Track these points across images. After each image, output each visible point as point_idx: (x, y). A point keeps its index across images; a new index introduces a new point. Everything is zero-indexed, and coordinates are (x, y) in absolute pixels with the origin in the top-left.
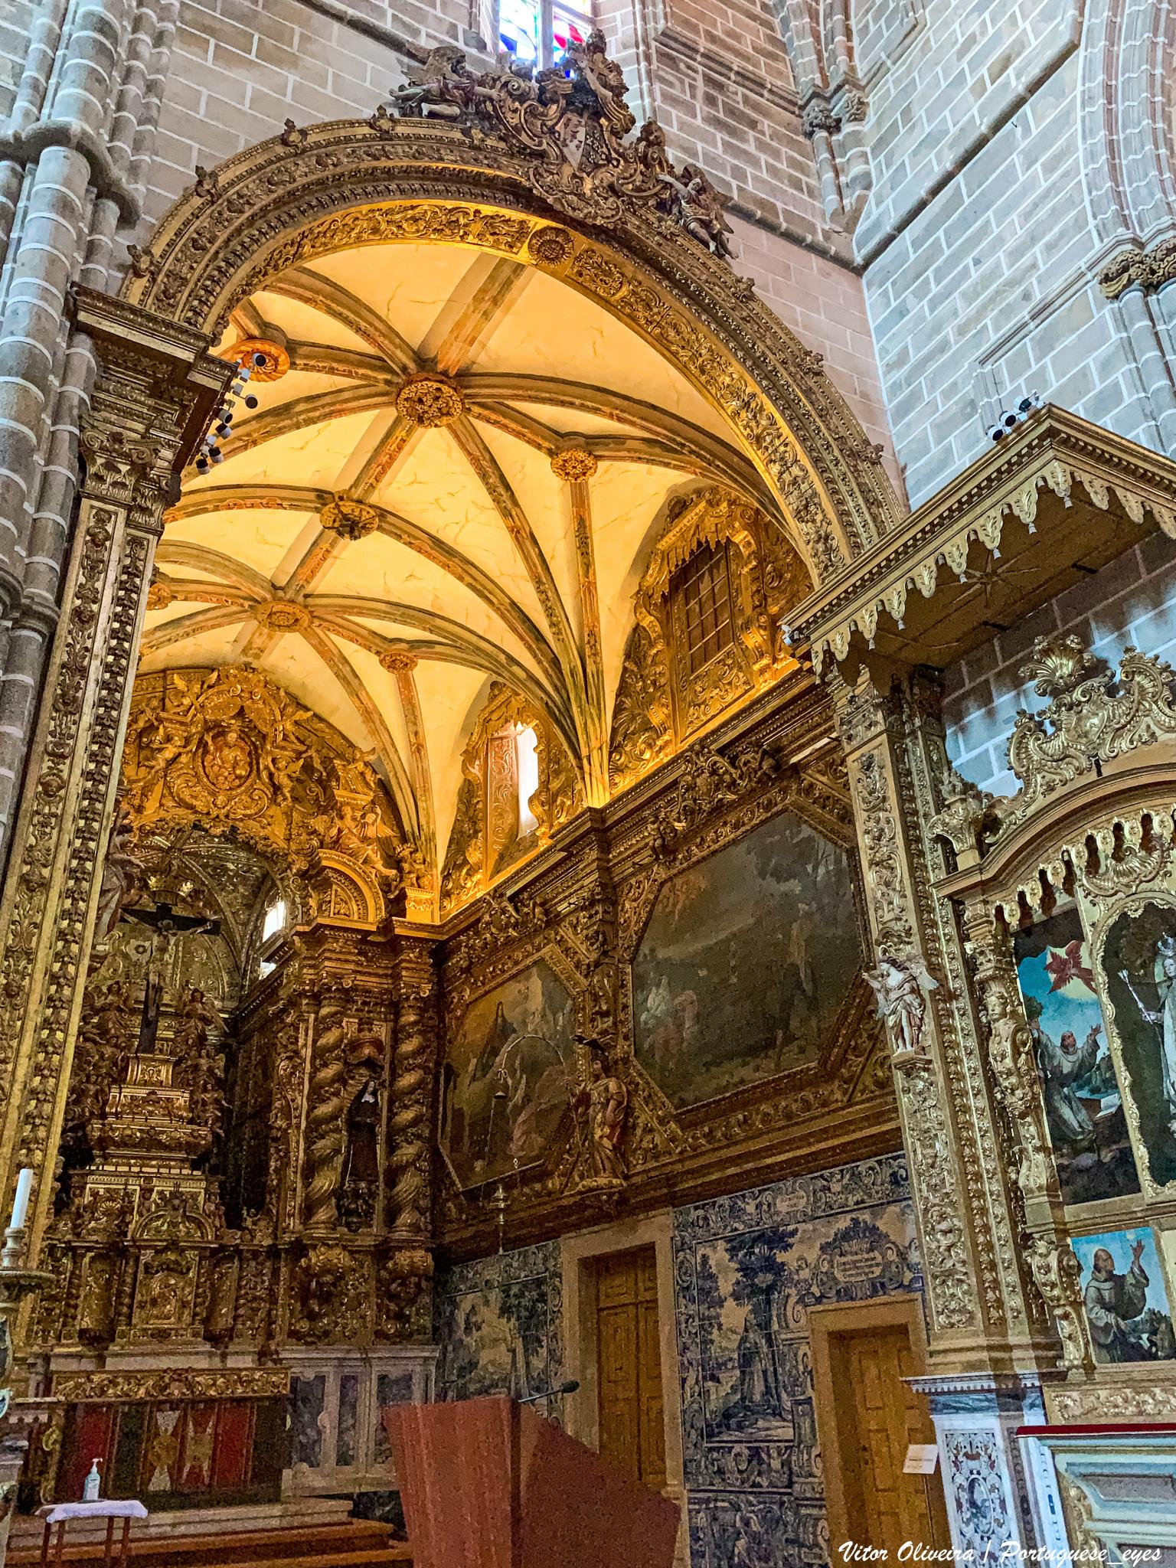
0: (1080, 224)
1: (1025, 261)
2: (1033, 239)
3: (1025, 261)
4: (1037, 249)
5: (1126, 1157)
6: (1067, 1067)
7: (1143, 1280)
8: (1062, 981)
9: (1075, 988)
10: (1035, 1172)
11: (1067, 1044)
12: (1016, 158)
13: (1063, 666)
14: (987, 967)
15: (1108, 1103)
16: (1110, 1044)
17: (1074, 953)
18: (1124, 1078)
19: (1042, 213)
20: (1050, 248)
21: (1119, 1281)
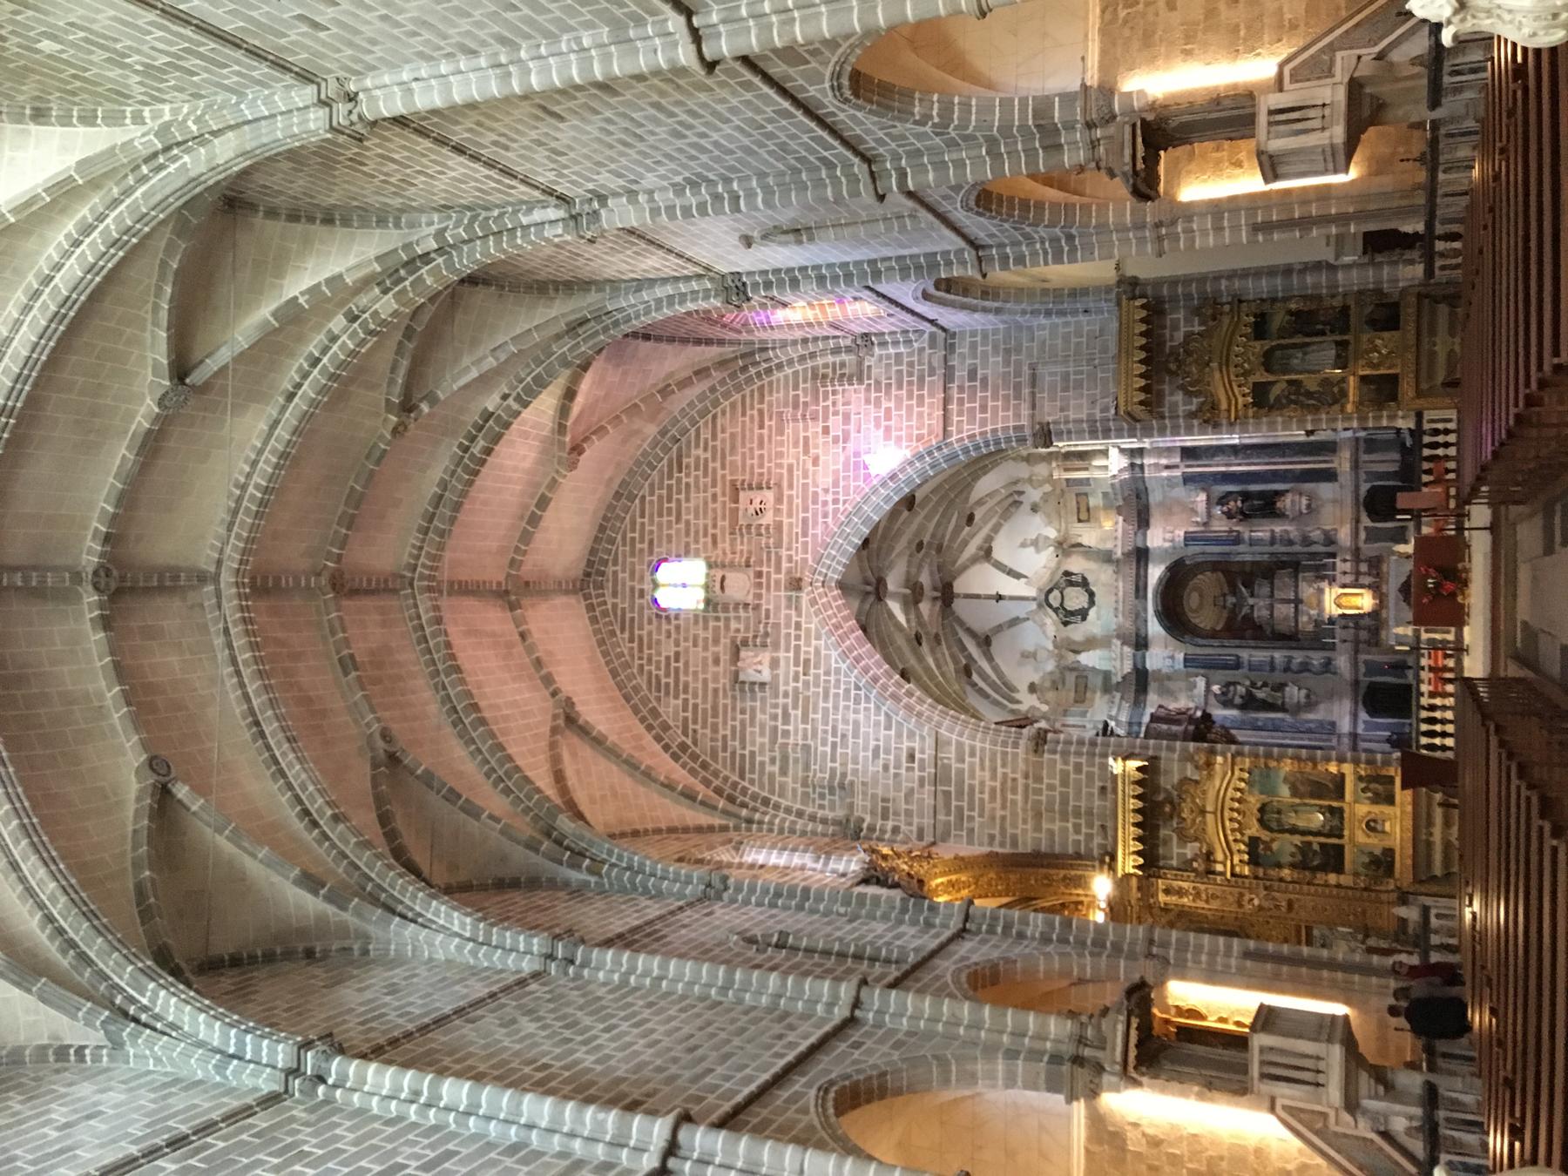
0: (1005, 754)
1: (999, 775)
2: (994, 770)
3: (999, 775)
4: (1000, 770)
5: (1334, 845)
6: (1299, 857)
7: (1371, 853)
8: (1270, 849)
9: (1275, 846)
10: (1332, 878)
11: (1293, 855)
12: (955, 765)
13: (1167, 809)
14: (1261, 872)
15: (1316, 847)
16: (1297, 839)
17: (1264, 842)
18: (1310, 838)
19: (987, 763)
20: (1004, 765)
21: (1372, 862)
